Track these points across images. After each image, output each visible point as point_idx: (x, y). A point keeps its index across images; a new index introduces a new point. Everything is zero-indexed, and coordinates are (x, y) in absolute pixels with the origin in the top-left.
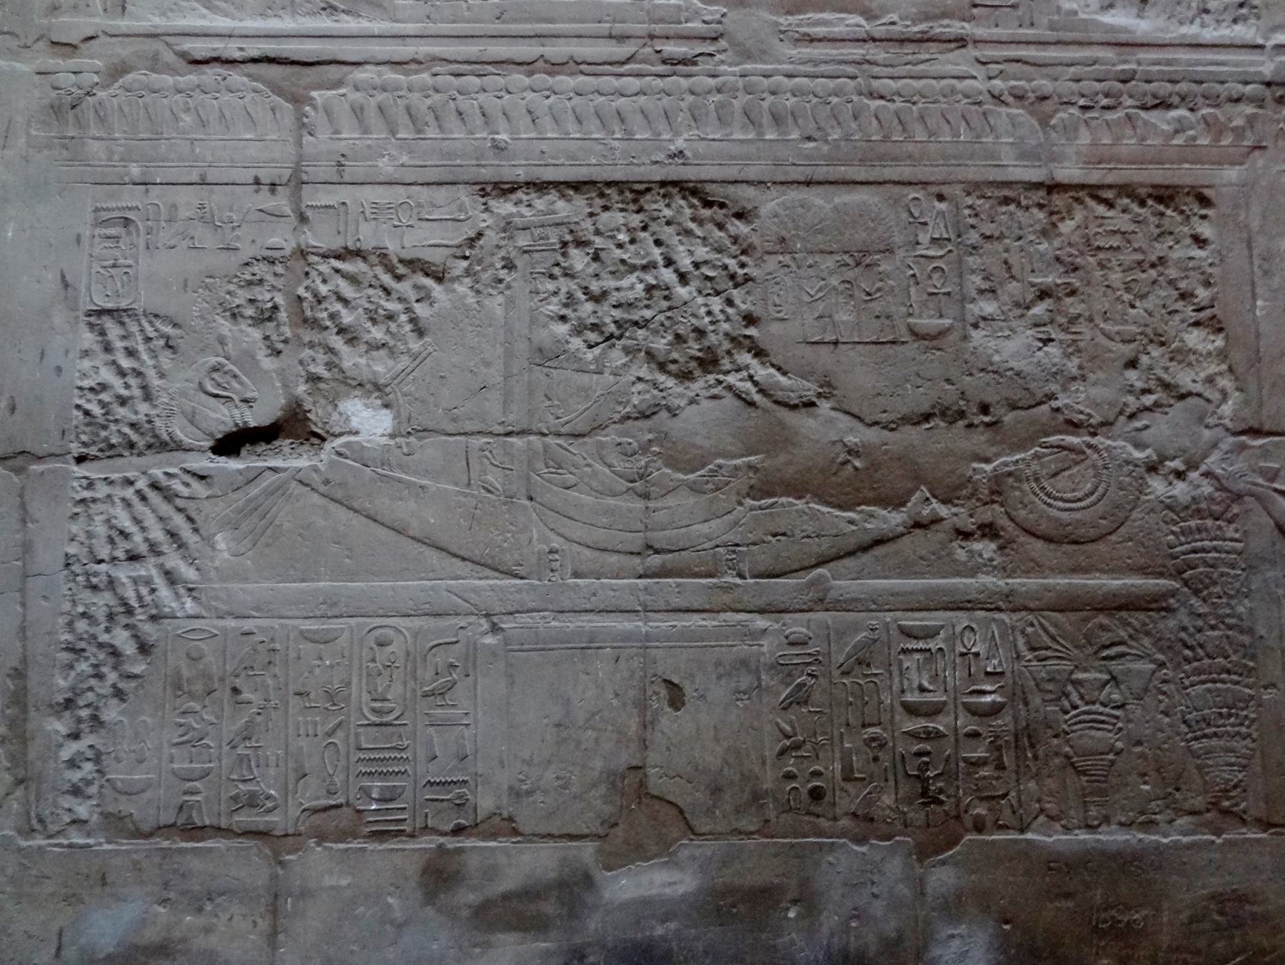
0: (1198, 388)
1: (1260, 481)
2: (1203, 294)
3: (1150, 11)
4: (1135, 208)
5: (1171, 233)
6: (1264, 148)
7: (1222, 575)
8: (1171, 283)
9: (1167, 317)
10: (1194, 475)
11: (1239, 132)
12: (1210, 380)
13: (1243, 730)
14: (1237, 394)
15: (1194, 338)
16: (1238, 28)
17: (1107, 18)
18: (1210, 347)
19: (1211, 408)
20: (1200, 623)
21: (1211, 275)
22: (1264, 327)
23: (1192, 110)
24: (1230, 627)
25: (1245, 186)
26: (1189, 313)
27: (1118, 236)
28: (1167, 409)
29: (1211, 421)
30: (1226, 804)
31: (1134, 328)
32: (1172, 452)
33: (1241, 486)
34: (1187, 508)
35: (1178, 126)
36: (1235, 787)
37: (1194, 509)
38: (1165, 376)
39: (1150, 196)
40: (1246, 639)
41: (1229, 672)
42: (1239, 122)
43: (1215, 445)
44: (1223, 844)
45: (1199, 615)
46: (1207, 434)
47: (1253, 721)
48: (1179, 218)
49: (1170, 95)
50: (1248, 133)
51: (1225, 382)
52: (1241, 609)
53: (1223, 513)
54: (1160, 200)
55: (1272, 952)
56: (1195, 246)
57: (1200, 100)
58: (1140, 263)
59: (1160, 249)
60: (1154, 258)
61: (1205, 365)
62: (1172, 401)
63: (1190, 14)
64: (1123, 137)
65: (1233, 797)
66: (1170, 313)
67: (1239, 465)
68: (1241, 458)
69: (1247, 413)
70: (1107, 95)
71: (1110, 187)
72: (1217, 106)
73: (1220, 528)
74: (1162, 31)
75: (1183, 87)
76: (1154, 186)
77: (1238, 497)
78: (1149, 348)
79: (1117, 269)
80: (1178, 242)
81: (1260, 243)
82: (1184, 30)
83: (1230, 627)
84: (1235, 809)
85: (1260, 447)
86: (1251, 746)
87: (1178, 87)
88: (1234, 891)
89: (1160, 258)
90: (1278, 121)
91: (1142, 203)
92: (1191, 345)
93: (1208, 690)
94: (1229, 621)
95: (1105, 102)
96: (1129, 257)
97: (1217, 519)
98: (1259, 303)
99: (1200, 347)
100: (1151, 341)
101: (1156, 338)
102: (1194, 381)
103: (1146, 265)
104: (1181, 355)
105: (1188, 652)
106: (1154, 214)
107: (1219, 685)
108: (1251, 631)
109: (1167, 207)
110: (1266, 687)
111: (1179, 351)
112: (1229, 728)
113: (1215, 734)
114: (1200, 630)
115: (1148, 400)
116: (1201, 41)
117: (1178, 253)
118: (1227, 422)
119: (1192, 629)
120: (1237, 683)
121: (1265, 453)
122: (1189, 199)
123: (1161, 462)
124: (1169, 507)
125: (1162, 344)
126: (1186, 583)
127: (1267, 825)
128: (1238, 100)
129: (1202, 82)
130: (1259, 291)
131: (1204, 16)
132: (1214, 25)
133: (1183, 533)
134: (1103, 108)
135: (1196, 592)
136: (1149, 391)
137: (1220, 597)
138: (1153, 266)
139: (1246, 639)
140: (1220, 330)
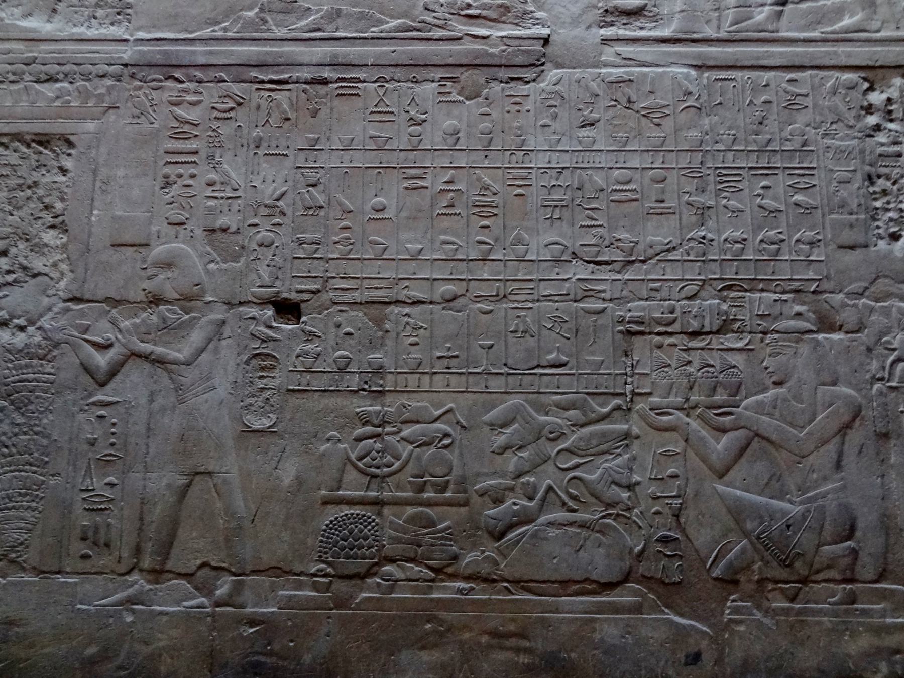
0: (46, 270)
1: (76, 334)
2: (59, 206)
3: (57, 18)
4: (24, 149)
5: (45, 166)
6: (118, 108)
7: (37, 397)
8: (40, 199)
9: (34, 222)
10: (31, 329)
11: (100, 98)
12: (55, 265)
13: (34, 504)
14: (70, 274)
15: (50, 237)
16: (112, 28)
17: (24, 23)
18: (58, 242)
19: (52, 283)
20: (16, 430)
21: (66, 193)
22: (93, 229)
23: (71, 83)
24: (36, 434)
25: (98, 136)
26: (49, 220)
27: (9, 168)
28: (23, 284)
29: (50, 292)
30: (14, 556)
31: (9, 229)
32: (20, 313)
33: (59, 336)
34: (21, 351)
35: (59, 94)
36: (21, 544)
37: (25, 352)
38: (25, 262)
39: (33, 141)
40: (45, 442)
41: (31, 465)
42: (102, 91)
43: (50, 309)
44: (5, 584)
45: (18, 425)
46: (46, 301)
47: (42, 498)
48: (52, 155)
49: (58, 74)
50: (107, 99)
51: (64, 267)
52: (45, 421)
53: (46, 355)
54: (40, 143)
55: (27, 660)
56: (60, 174)
57: (77, 76)
58: (20, 185)
59: (36, 176)
60: (30, 182)
61: (54, 254)
62: (27, 279)
63: (82, 19)
64: (21, 101)
65: (19, 551)
66: (35, 219)
67: (63, 322)
68: (65, 317)
69: (74, 287)
70: (14, 74)
71: (5, 134)
72: (89, 80)
73: (42, 365)
74: (60, 31)
75: (67, 68)
76: (36, 134)
77: (57, 345)
78: (18, 243)
79: (5, 189)
80: (48, 171)
81: (103, 172)
82: (75, 30)
83: (36, 434)
84: (19, 559)
85: (78, 310)
86: (37, 515)
87: (63, 68)
88: (7, 617)
89: (35, 182)
90: (129, 90)
91: (28, 146)
92: (46, 240)
93: (15, 477)
94: (36, 429)
95: (12, 78)
96: (13, 182)
97: (41, 359)
98: (95, 212)
99: (52, 242)
100: (21, 238)
101: (23, 236)
102: (45, 265)
103: (24, 187)
104: (39, 248)
105: (5, 450)
106: (34, 153)
107: (23, 473)
108: (48, 437)
109: (46, 148)
110: (53, 475)
111: (36, 245)
112: (24, 503)
113: (14, 508)
114: (16, 435)
115: (10, 278)
116: (83, 37)
117: (48, 178)
118: (60, 293)
119: (10, 435)
120: (34, 472)
121: (82, 314)
122: (59, 143)
123: (11, 320)
124: (9, 351)
125: (27, 240)
126: (12, 403)
127: (38, 571)
128: (103, 76)
129: (81, 64)
130: (96, 204)
131: (93, 20)
132: (97, 25)
133: (15, 368)
134: (10, 82)
135: (18, 409)
136: (13, 272)
137: (33, 413)
138: (29, 187)
139: (45, 442)
140: (67, 230)
